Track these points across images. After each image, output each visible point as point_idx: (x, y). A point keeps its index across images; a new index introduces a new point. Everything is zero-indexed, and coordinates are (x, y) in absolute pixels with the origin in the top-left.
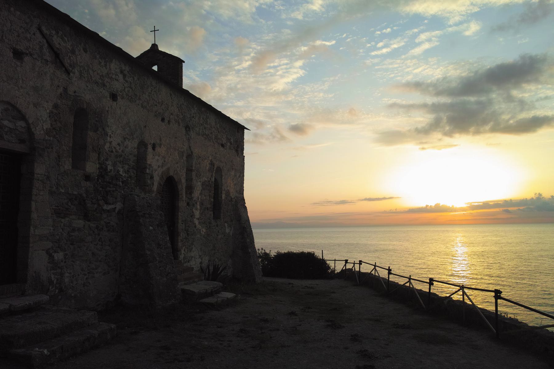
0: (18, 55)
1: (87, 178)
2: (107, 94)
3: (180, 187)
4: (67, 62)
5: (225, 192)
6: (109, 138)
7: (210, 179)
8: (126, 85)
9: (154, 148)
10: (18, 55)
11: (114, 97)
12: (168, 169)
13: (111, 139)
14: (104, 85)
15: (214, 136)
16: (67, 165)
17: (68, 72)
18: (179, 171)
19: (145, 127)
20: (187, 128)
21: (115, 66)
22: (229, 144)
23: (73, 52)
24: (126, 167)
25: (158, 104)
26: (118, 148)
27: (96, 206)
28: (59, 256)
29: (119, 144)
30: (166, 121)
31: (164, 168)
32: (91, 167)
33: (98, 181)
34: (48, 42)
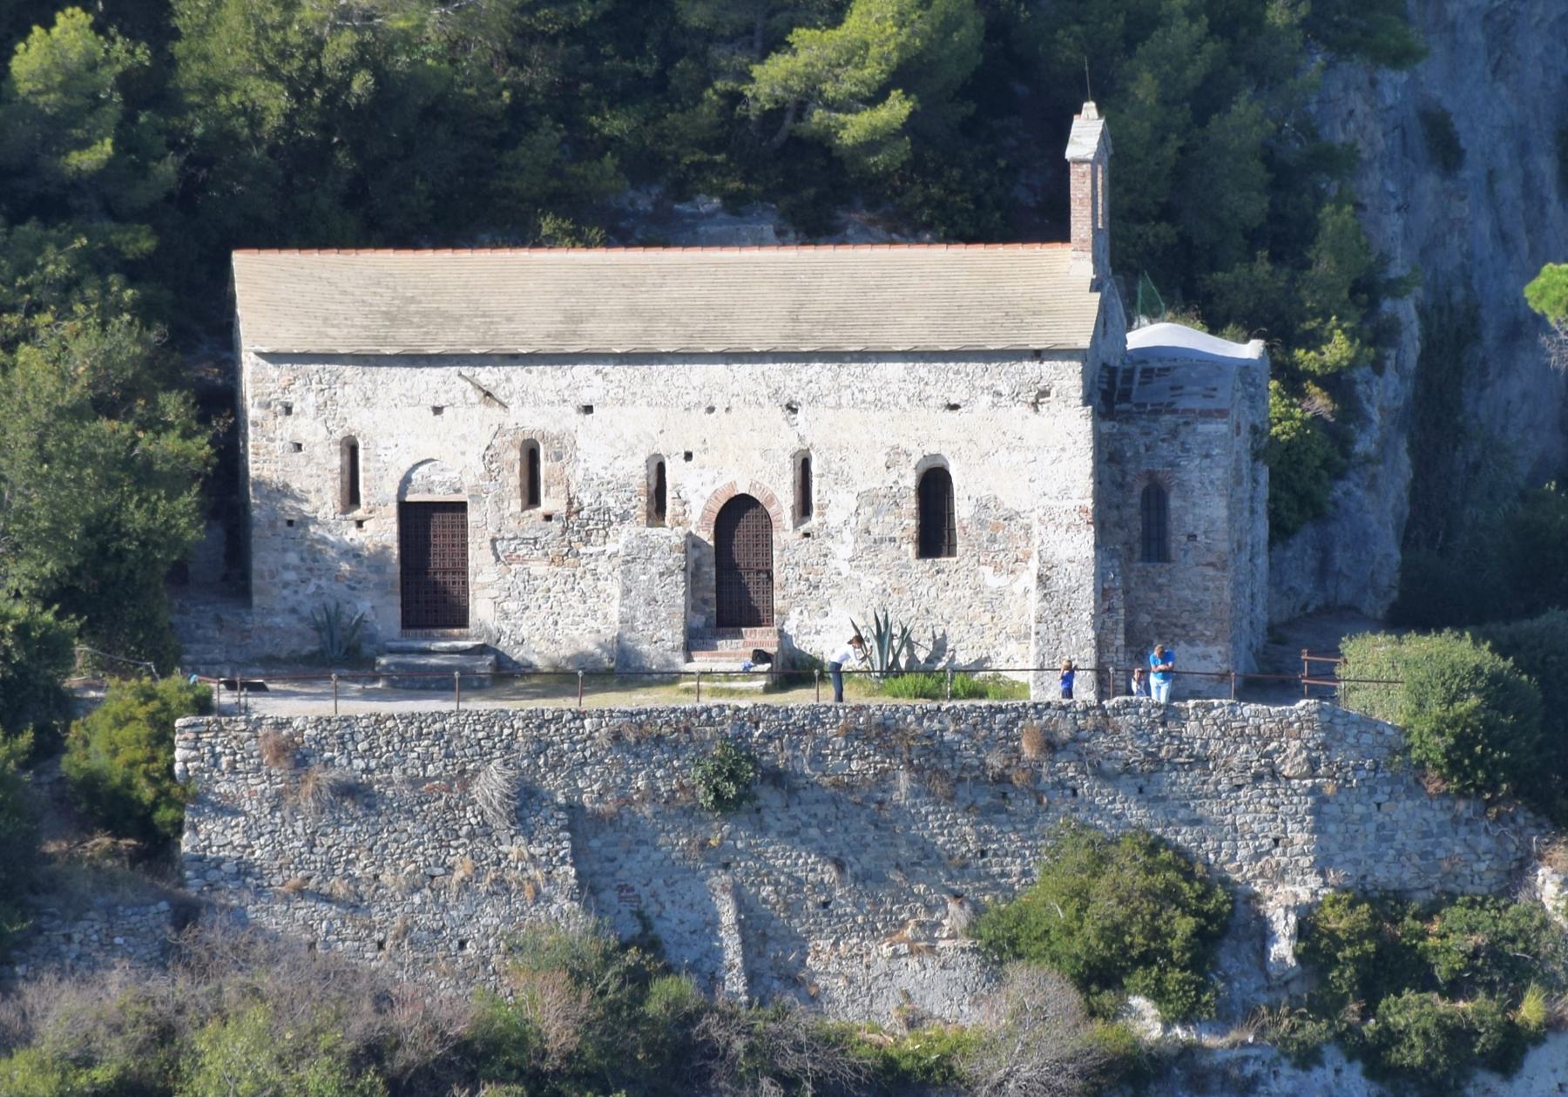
0: (438, 410)
1: (548, 518)
2: (570, 410)
3: (771, 510)
4: (500, 394)
5: (973, 501)
6: (582, 464)
7: (896, 482)
8: (610, 386)
9: (688, 456)
10: (438, 410)
11: (588, 409)
12: (732, 485)
13: (588, 465)
14: (565, 401)
15: (903, 400)
16: (516, 504)
17: (504, 406)
18: (766, 484)
19: (661, 432)
20: (792, 408)
21: (583, 371)
22: (987, 399)
23: (508, 380)
24: (623, 496)
25: (692, 391)
26: (602, 473)
27: (566, 550)
28: (511, 606)
29: (606, 468)
30: (719, 410)
31: (719, 485)
32: (551, 502)
33: (567, 518)
34: (472, 383)
